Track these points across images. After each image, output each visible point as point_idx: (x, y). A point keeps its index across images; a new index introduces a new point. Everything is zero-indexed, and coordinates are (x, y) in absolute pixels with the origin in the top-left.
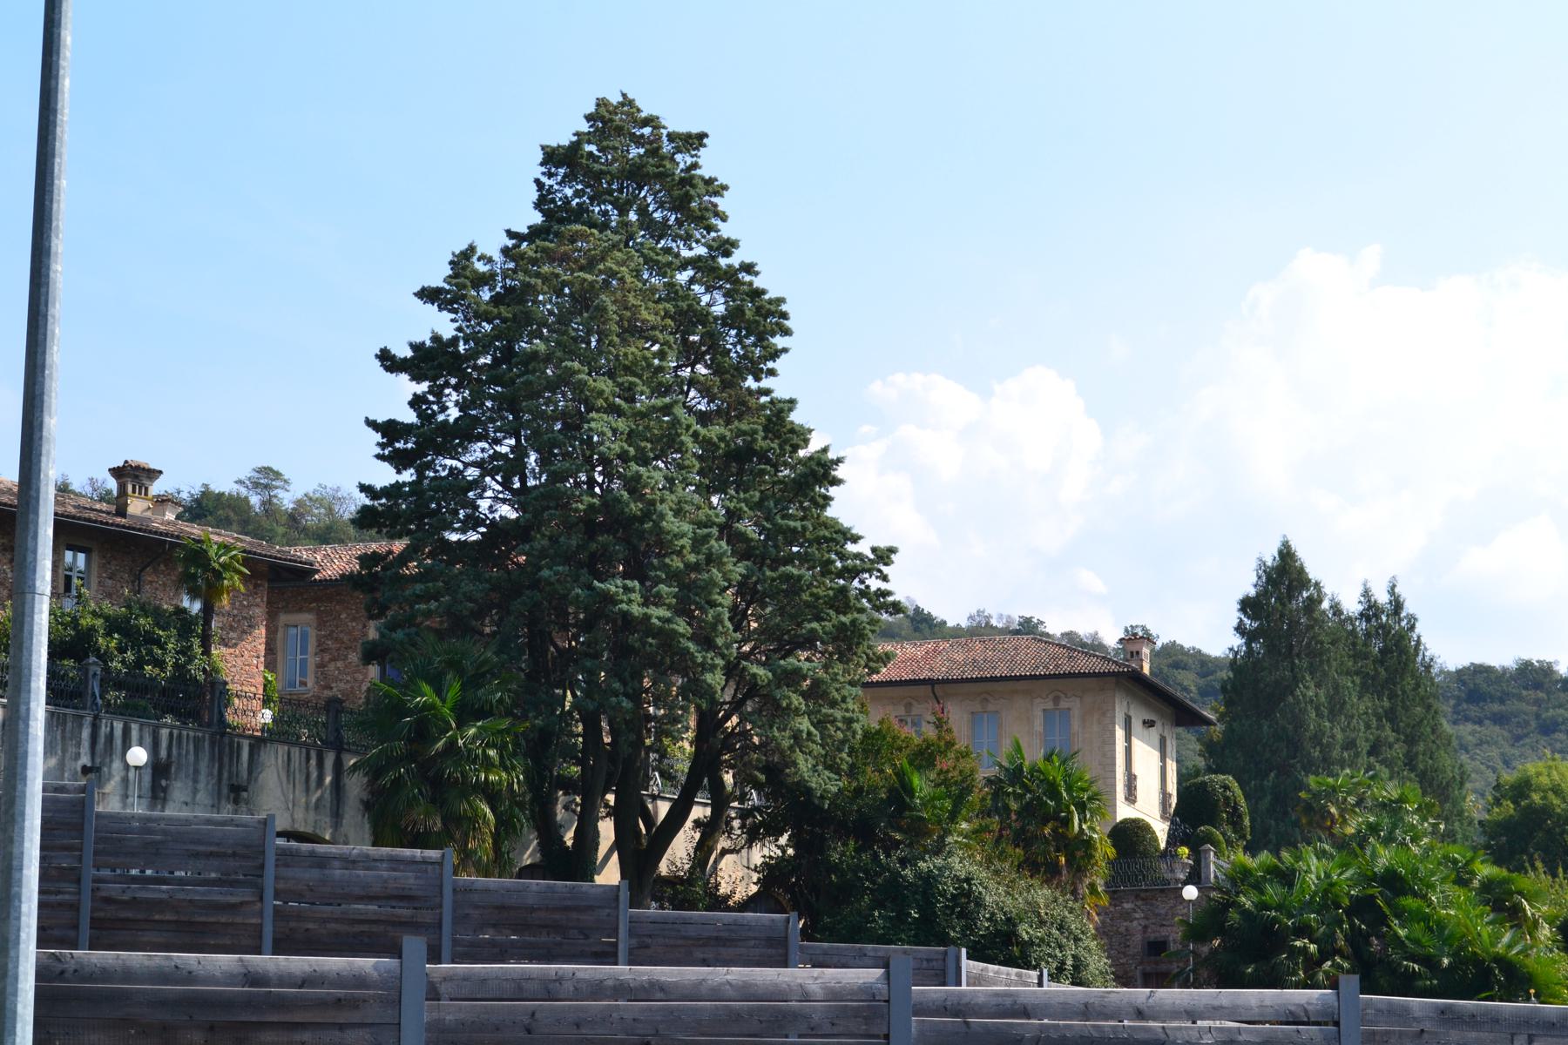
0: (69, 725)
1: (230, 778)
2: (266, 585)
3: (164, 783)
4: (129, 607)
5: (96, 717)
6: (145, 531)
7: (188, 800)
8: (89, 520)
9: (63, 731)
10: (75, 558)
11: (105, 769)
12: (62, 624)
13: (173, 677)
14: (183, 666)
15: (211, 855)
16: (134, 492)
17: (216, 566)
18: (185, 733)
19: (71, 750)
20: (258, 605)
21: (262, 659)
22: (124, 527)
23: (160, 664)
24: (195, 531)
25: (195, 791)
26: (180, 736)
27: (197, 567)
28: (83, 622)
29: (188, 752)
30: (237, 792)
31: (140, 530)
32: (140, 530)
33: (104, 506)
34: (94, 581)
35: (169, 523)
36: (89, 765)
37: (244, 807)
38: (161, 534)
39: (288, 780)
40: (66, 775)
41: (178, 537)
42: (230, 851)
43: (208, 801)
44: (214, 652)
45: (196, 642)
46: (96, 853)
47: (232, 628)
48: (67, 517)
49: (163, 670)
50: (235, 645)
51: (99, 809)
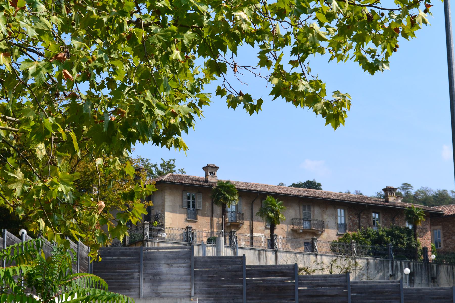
0: (385, 263)
1: (431, 275)
2: (429, 219)
3: (413, 278)
4: (392, 228)
5: (392, 261)
6: (394, 206)
7: (420, 282)
8: (379, 204)
9: (384, 265)
10: (375, 215)
11: (396, 275)
12: (374, 234)
13: (407, 247)
14: (409, 244)
15: (437, 298)
16: (390, 195)
17: (416, 214)
18: (417, 263)
19: (386, 270)
20: (428, 225)
21: (430, 240)
22: (388, 205)
23: (402, 244)
24: (408, 205)
25: (422, 280)
26: (416, 264)
27: (411, 215)
28: (380, 233)
29: (419, 269)
30: (433, 279)
31: (393, 206)
32: (393, 206)
33: (381, 200)
34: (381, 221)
35: (400, 203)
36: (392, 274)
37: (436, 284)
38: (399, 206)
39: (448, 275)
40: (386, 277)
41: (404, 207)
42: (443, 297)
43: (426, 283)
44: (417, 239)
45: (412, 237)
46: (405, 299)
47: (421, 232)
48: (373, 204)
49: (404, 245)
50: (422, 237)
51: (404, 287)
